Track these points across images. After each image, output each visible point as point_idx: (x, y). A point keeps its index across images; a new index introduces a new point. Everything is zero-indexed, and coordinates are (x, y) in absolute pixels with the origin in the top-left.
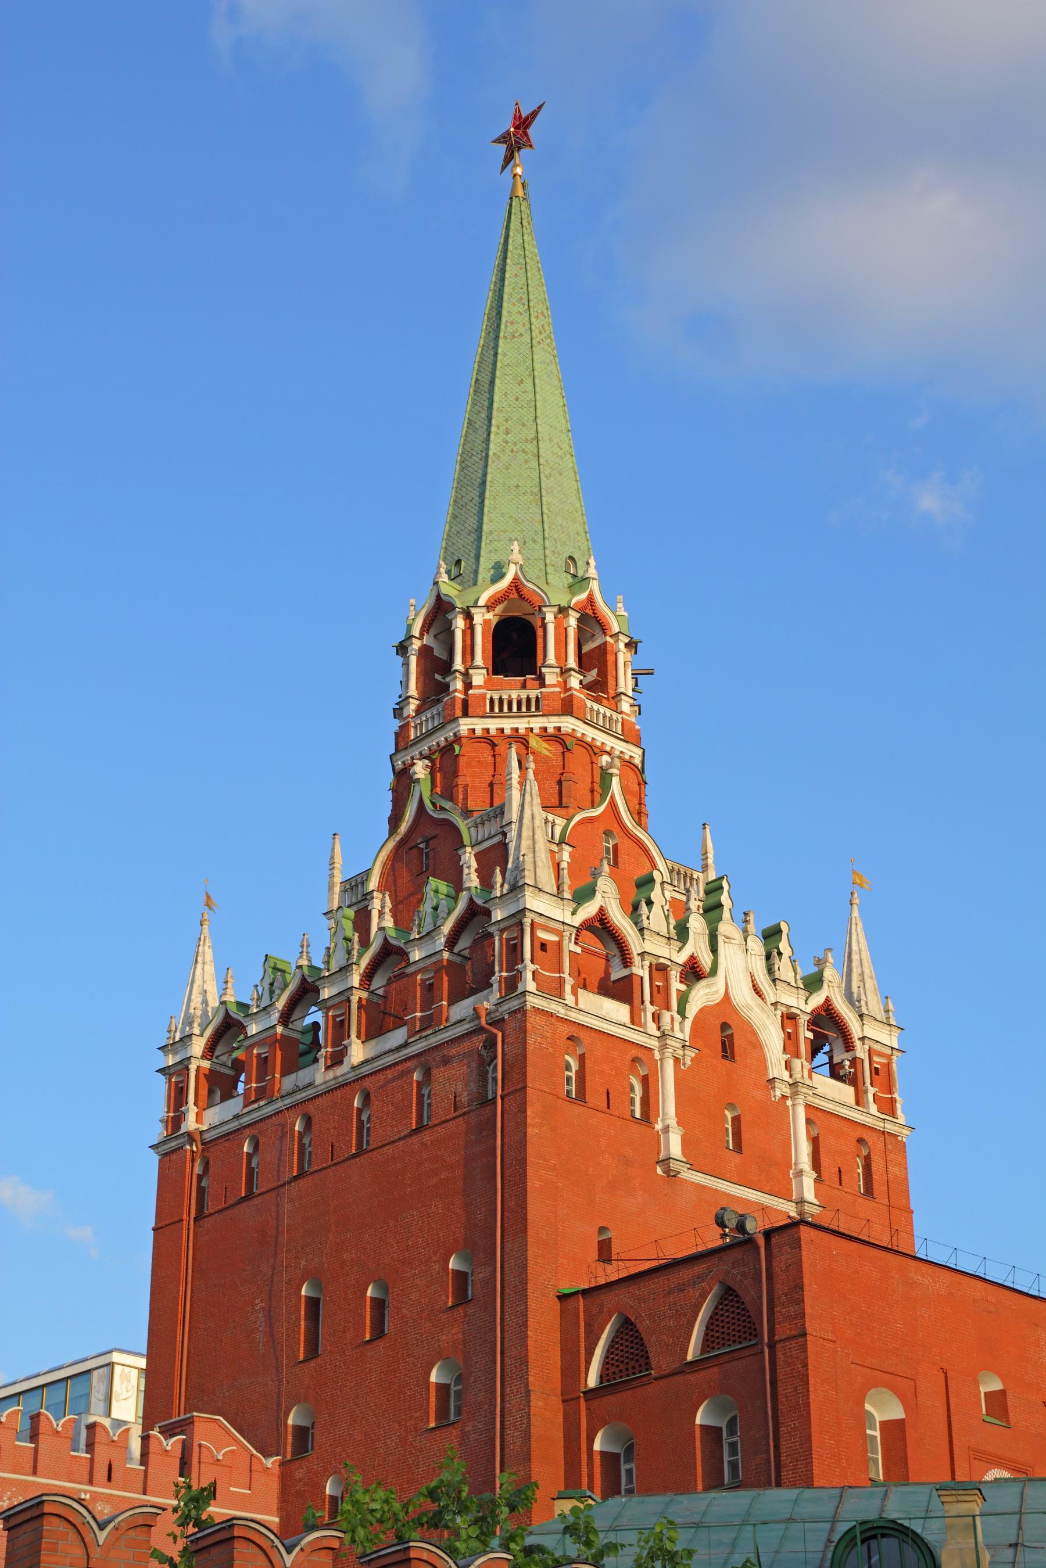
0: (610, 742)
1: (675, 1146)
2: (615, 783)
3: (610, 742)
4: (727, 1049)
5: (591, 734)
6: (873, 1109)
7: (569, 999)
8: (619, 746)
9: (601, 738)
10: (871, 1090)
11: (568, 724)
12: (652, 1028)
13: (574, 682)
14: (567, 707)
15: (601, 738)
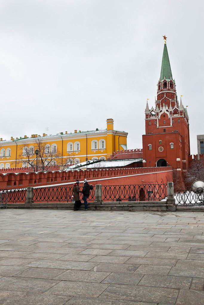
0: (166, 92)
1: (158, 125)
2: (165, 95)
3: (166, 92)
4: (164, 116)
5: (164, 92)
6: (180, 115)
7: (149, 118)
8: (167, 91)
9: (165, 92)
10: (180, 114)
11: (161, 92)
12: (156, 117)
13: (162, 88)
14: (161, 91)
15: (165, 92)
